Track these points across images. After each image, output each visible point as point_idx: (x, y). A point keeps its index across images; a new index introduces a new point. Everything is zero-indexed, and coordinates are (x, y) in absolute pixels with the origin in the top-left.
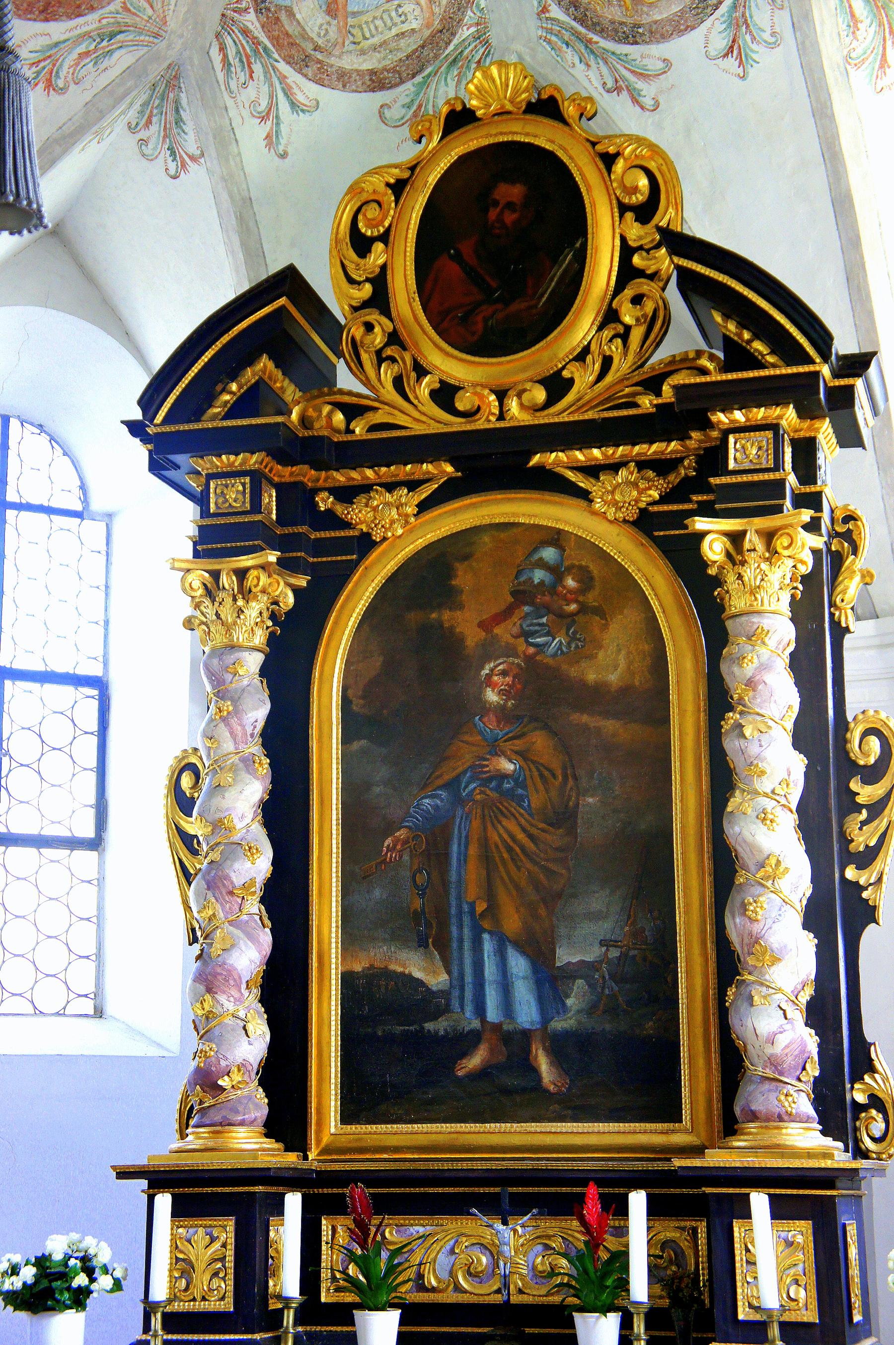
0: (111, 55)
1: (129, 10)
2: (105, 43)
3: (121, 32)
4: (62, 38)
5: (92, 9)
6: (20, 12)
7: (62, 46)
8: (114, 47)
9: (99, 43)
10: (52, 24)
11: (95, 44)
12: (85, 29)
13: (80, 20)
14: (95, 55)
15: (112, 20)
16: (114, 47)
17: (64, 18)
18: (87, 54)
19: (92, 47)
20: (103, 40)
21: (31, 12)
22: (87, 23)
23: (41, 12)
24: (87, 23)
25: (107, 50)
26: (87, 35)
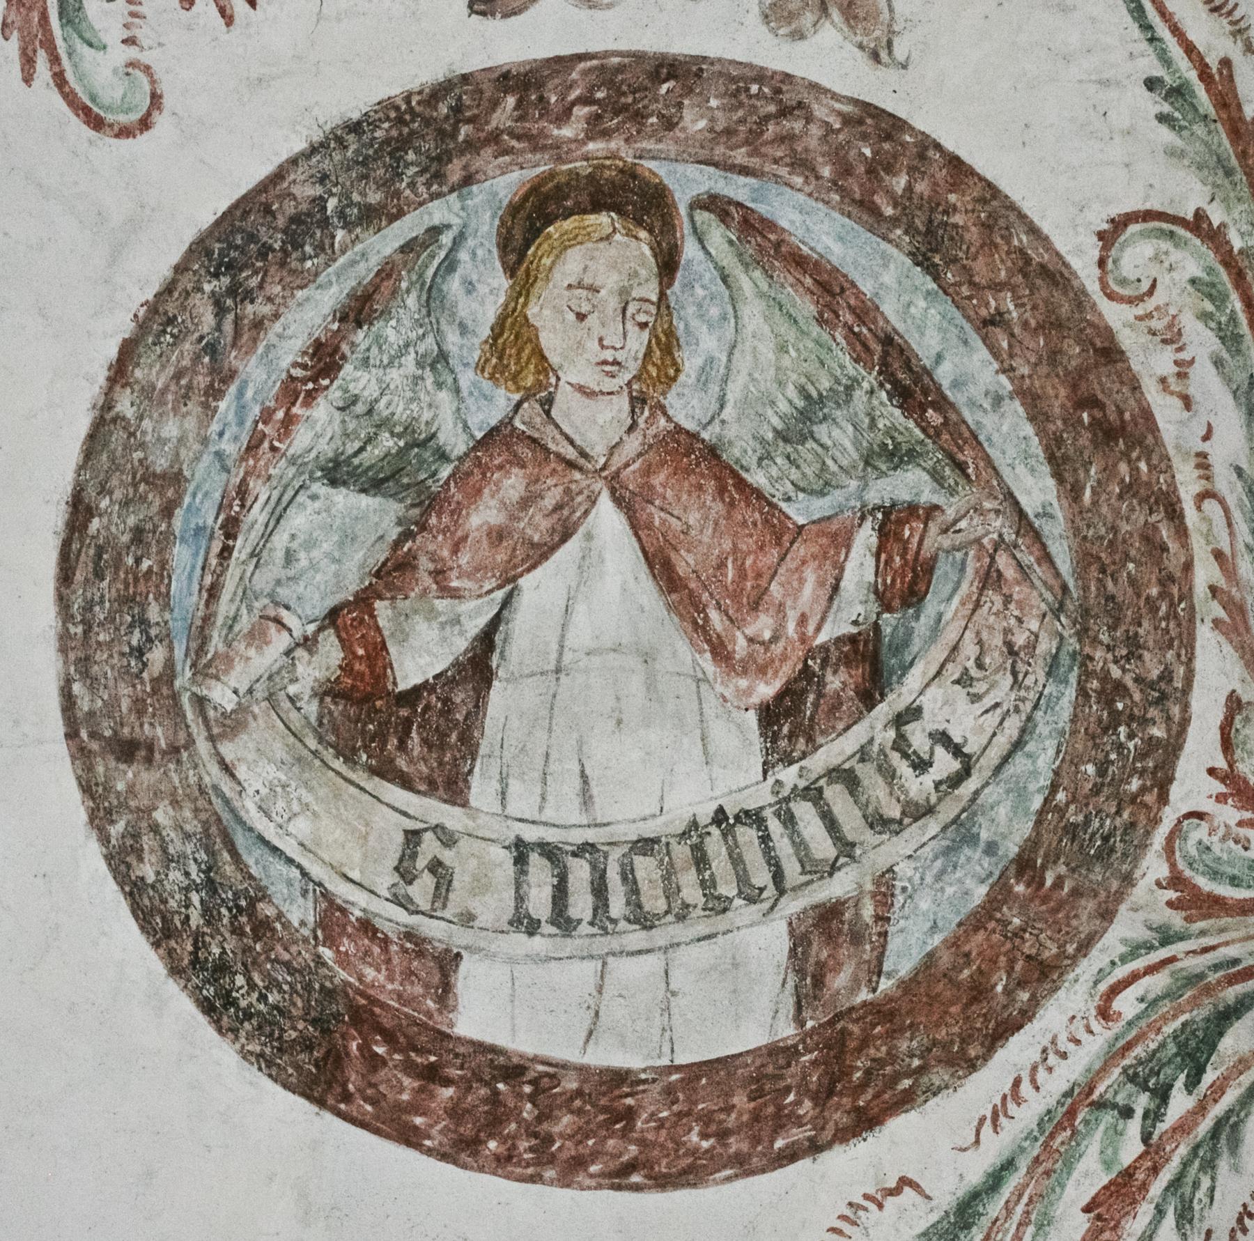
0: (1235, 1144)
1: (1215, 905)
2: (1180, 1103)
3: (1226, 1017)
4: (976, 1169)
5: (1044, 974)
6: (736, 1144)
7: (994, 1207)
8: (1230, 1097)
9: (1152, 1116)
10: (899, 1126)
11: (1134, 1127)
12: (1058, 1081)
13: (1018, 1051)
14: (1166, 1176)
15: (1157, 983)
16: (1230, 1097)
17: (939, 1075)
18: (1122, 1190)
19: (1131, 1149)
20: (1162, 1095)
21: (782, 1120)
22: (1052, 1051)
23: (823, 1096)
24: (1052, 1051)
25: (1205, 1126)
26: (1080, 1102)
